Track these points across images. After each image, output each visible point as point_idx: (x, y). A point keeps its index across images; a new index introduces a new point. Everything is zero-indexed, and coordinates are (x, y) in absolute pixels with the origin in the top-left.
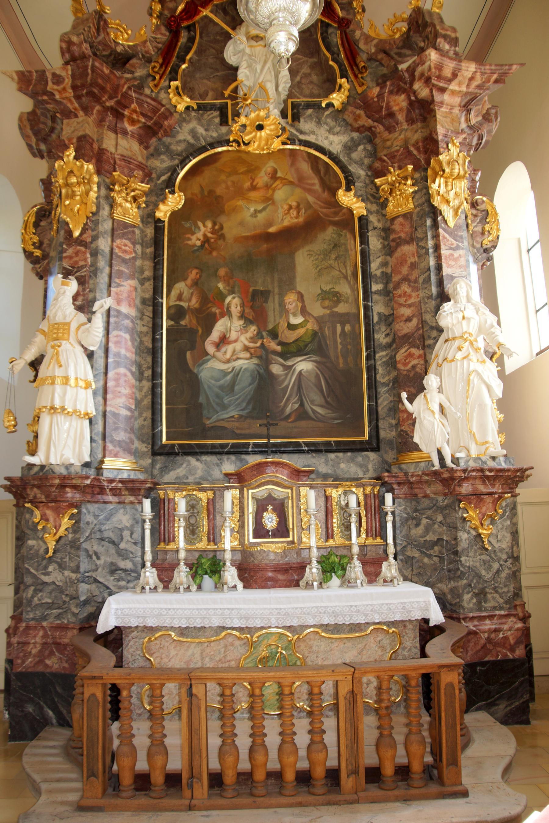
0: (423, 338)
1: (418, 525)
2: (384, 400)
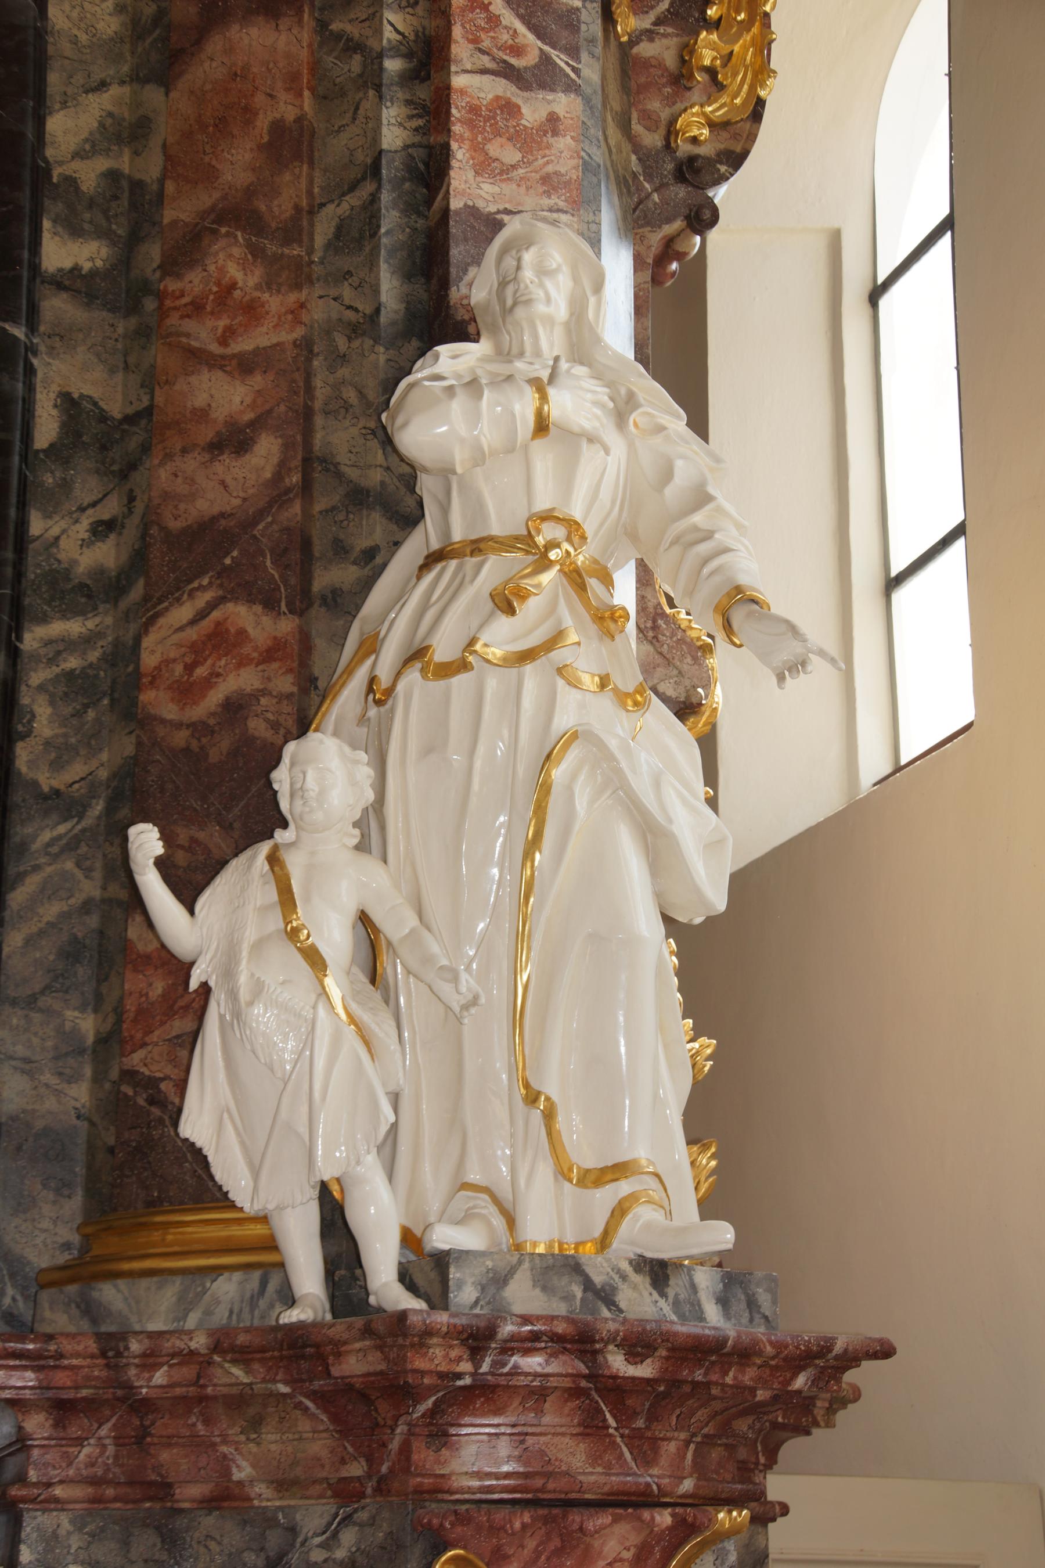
0: (300, 552)
2: (48, 892)
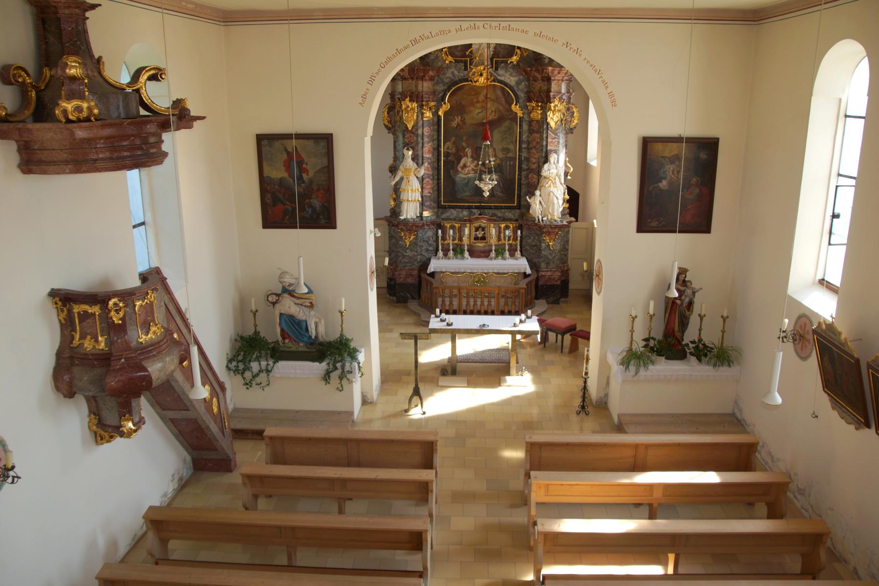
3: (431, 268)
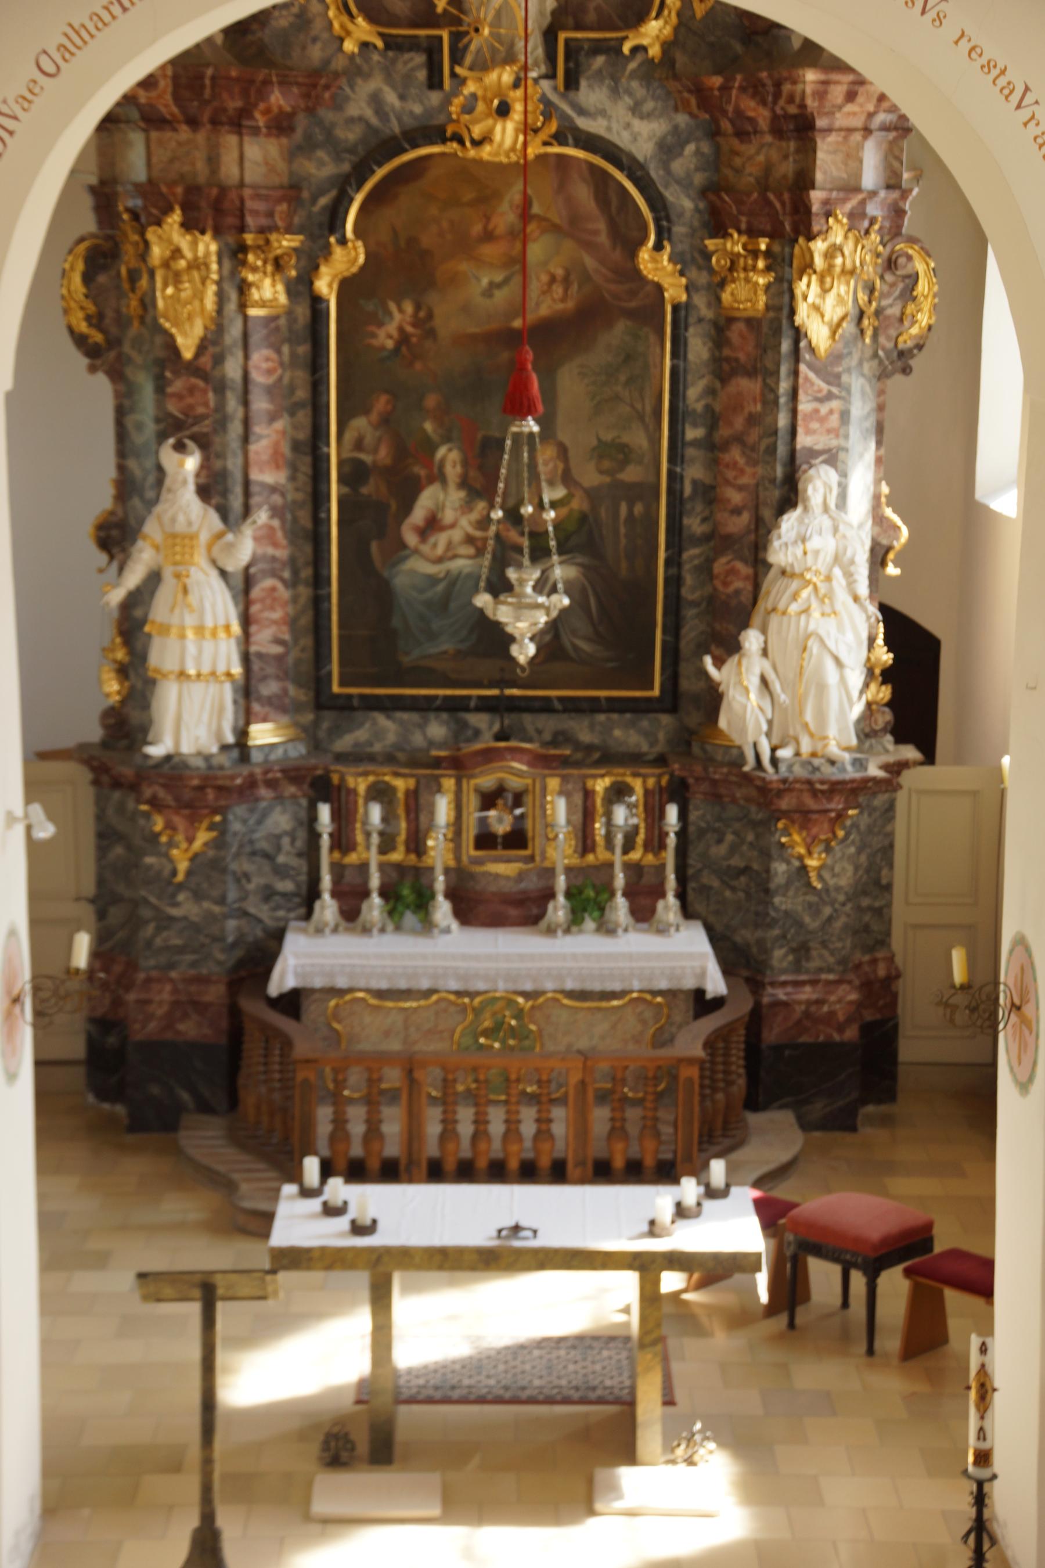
1: (720, 841)
3: (287, 974)
